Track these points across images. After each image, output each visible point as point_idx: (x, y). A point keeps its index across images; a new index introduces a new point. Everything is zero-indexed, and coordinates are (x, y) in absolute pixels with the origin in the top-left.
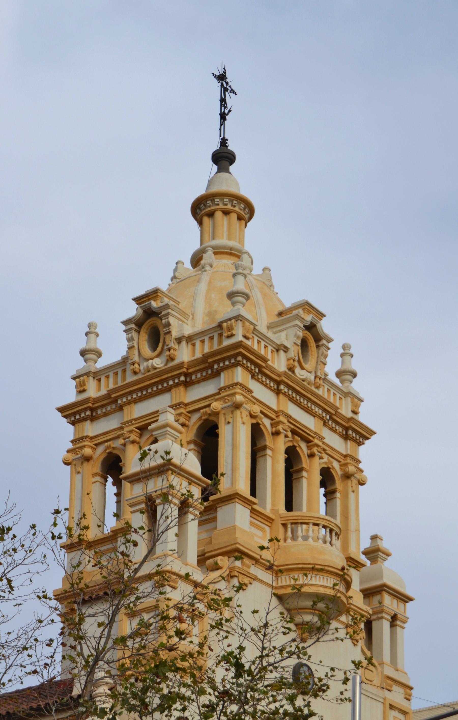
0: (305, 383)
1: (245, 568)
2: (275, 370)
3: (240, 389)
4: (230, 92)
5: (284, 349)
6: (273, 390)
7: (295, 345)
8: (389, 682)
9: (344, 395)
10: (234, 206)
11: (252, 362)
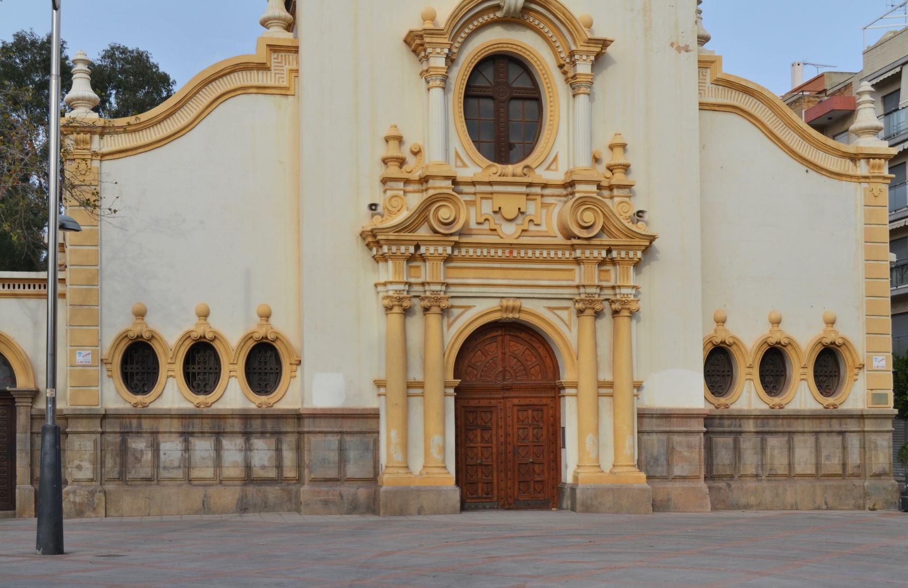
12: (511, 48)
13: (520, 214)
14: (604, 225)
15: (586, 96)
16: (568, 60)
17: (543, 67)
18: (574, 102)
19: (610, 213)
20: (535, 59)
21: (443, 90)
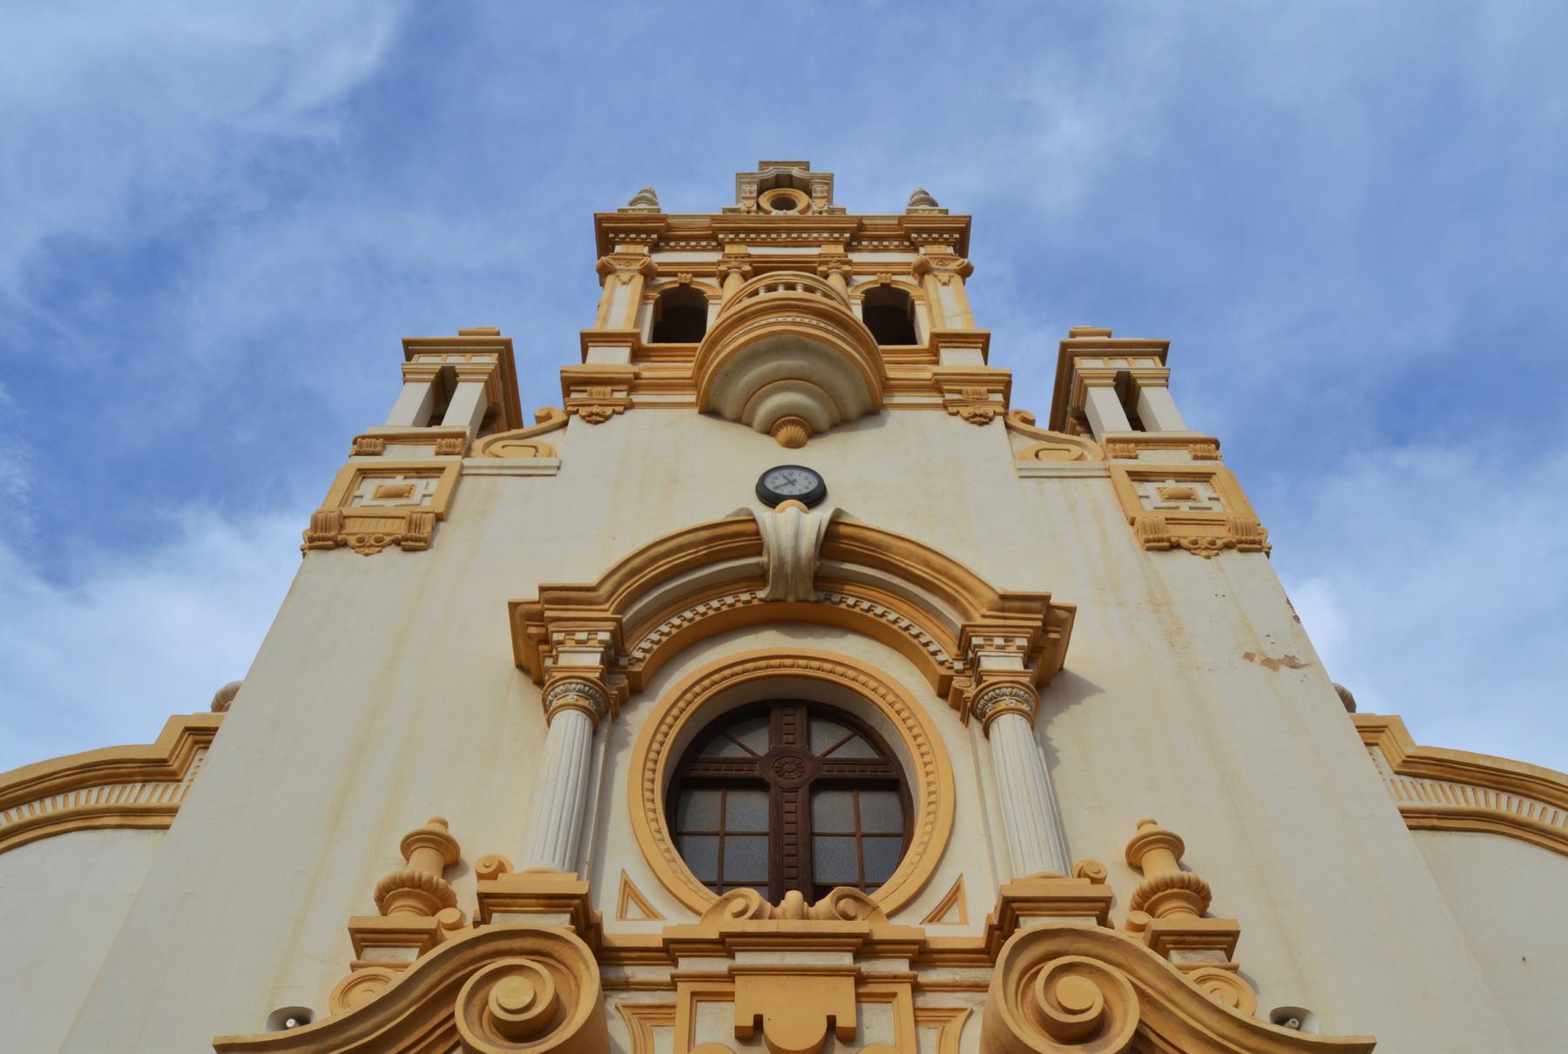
11: (638, 231)
12: (806, 667)
13: (838, 1044)
14: (1154, 1021)
15: (1017, 717)
16: (959, 665)
17: (897, 696)
18: (989, 749)
19: (1162, 986)
20: (873, 684)
21: (588, 723)
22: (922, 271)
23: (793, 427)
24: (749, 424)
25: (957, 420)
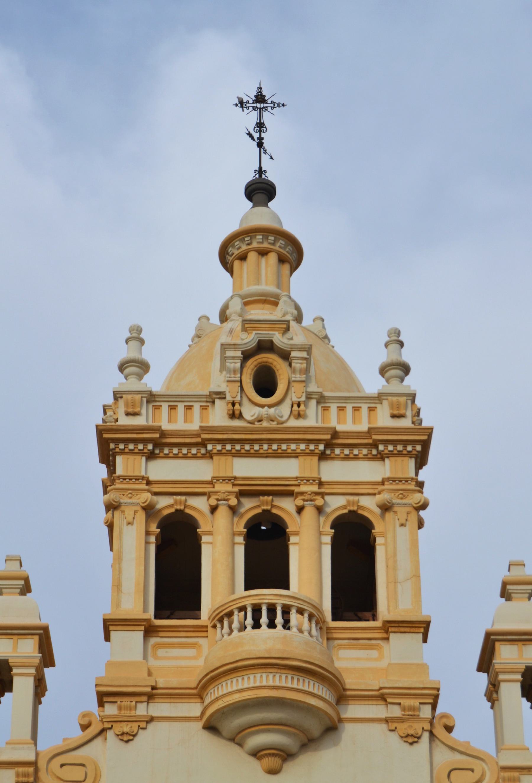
0: (265, 424)
1: (128, 713)
2: (186, 433)
3: (122, 483)
4: (272, 108)
5: (218, 396)
6: (203, 457)
7: (230, 384)
8: (507, 774)
9: (377, 401)
10: (239, 248)
22: (386, 508)
23: (273, 758)
24: (240, 745)
25: (394, 738)
